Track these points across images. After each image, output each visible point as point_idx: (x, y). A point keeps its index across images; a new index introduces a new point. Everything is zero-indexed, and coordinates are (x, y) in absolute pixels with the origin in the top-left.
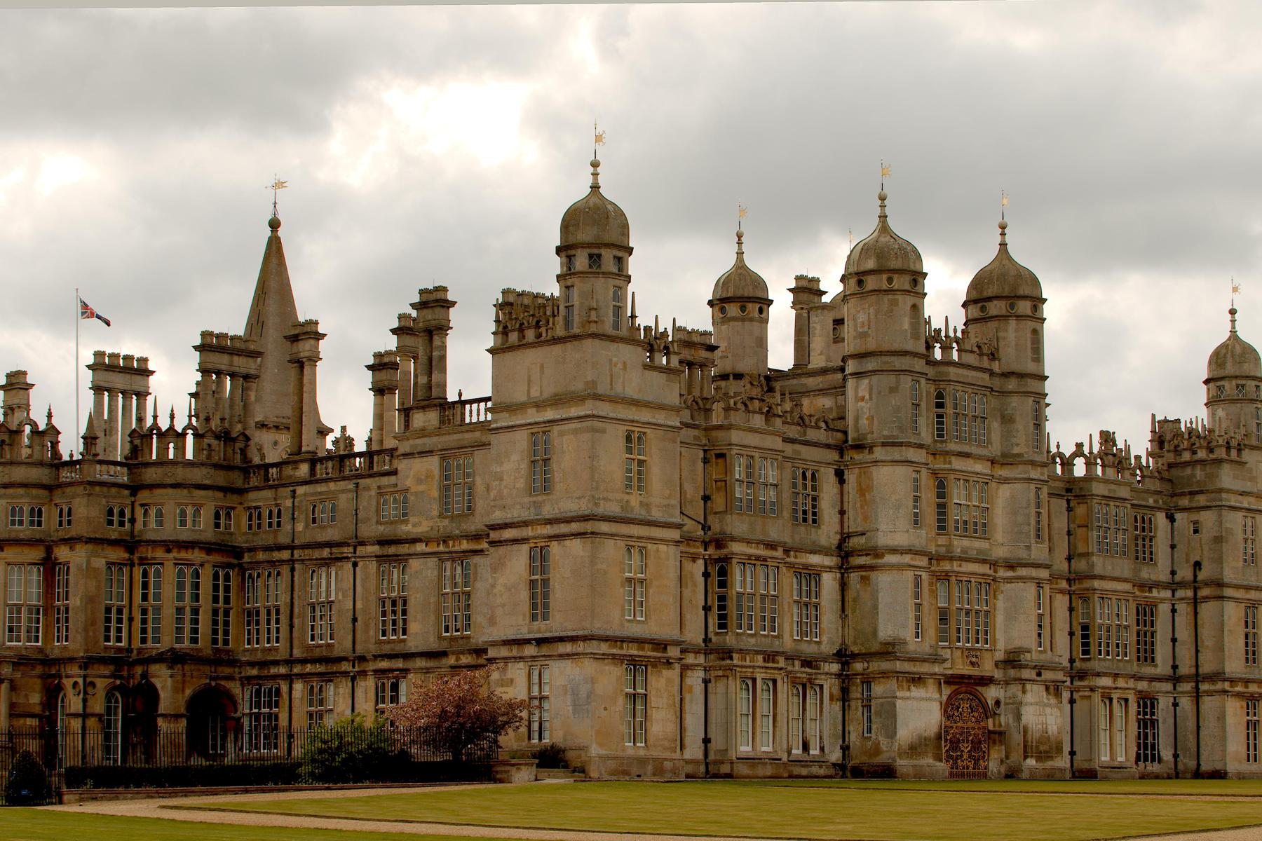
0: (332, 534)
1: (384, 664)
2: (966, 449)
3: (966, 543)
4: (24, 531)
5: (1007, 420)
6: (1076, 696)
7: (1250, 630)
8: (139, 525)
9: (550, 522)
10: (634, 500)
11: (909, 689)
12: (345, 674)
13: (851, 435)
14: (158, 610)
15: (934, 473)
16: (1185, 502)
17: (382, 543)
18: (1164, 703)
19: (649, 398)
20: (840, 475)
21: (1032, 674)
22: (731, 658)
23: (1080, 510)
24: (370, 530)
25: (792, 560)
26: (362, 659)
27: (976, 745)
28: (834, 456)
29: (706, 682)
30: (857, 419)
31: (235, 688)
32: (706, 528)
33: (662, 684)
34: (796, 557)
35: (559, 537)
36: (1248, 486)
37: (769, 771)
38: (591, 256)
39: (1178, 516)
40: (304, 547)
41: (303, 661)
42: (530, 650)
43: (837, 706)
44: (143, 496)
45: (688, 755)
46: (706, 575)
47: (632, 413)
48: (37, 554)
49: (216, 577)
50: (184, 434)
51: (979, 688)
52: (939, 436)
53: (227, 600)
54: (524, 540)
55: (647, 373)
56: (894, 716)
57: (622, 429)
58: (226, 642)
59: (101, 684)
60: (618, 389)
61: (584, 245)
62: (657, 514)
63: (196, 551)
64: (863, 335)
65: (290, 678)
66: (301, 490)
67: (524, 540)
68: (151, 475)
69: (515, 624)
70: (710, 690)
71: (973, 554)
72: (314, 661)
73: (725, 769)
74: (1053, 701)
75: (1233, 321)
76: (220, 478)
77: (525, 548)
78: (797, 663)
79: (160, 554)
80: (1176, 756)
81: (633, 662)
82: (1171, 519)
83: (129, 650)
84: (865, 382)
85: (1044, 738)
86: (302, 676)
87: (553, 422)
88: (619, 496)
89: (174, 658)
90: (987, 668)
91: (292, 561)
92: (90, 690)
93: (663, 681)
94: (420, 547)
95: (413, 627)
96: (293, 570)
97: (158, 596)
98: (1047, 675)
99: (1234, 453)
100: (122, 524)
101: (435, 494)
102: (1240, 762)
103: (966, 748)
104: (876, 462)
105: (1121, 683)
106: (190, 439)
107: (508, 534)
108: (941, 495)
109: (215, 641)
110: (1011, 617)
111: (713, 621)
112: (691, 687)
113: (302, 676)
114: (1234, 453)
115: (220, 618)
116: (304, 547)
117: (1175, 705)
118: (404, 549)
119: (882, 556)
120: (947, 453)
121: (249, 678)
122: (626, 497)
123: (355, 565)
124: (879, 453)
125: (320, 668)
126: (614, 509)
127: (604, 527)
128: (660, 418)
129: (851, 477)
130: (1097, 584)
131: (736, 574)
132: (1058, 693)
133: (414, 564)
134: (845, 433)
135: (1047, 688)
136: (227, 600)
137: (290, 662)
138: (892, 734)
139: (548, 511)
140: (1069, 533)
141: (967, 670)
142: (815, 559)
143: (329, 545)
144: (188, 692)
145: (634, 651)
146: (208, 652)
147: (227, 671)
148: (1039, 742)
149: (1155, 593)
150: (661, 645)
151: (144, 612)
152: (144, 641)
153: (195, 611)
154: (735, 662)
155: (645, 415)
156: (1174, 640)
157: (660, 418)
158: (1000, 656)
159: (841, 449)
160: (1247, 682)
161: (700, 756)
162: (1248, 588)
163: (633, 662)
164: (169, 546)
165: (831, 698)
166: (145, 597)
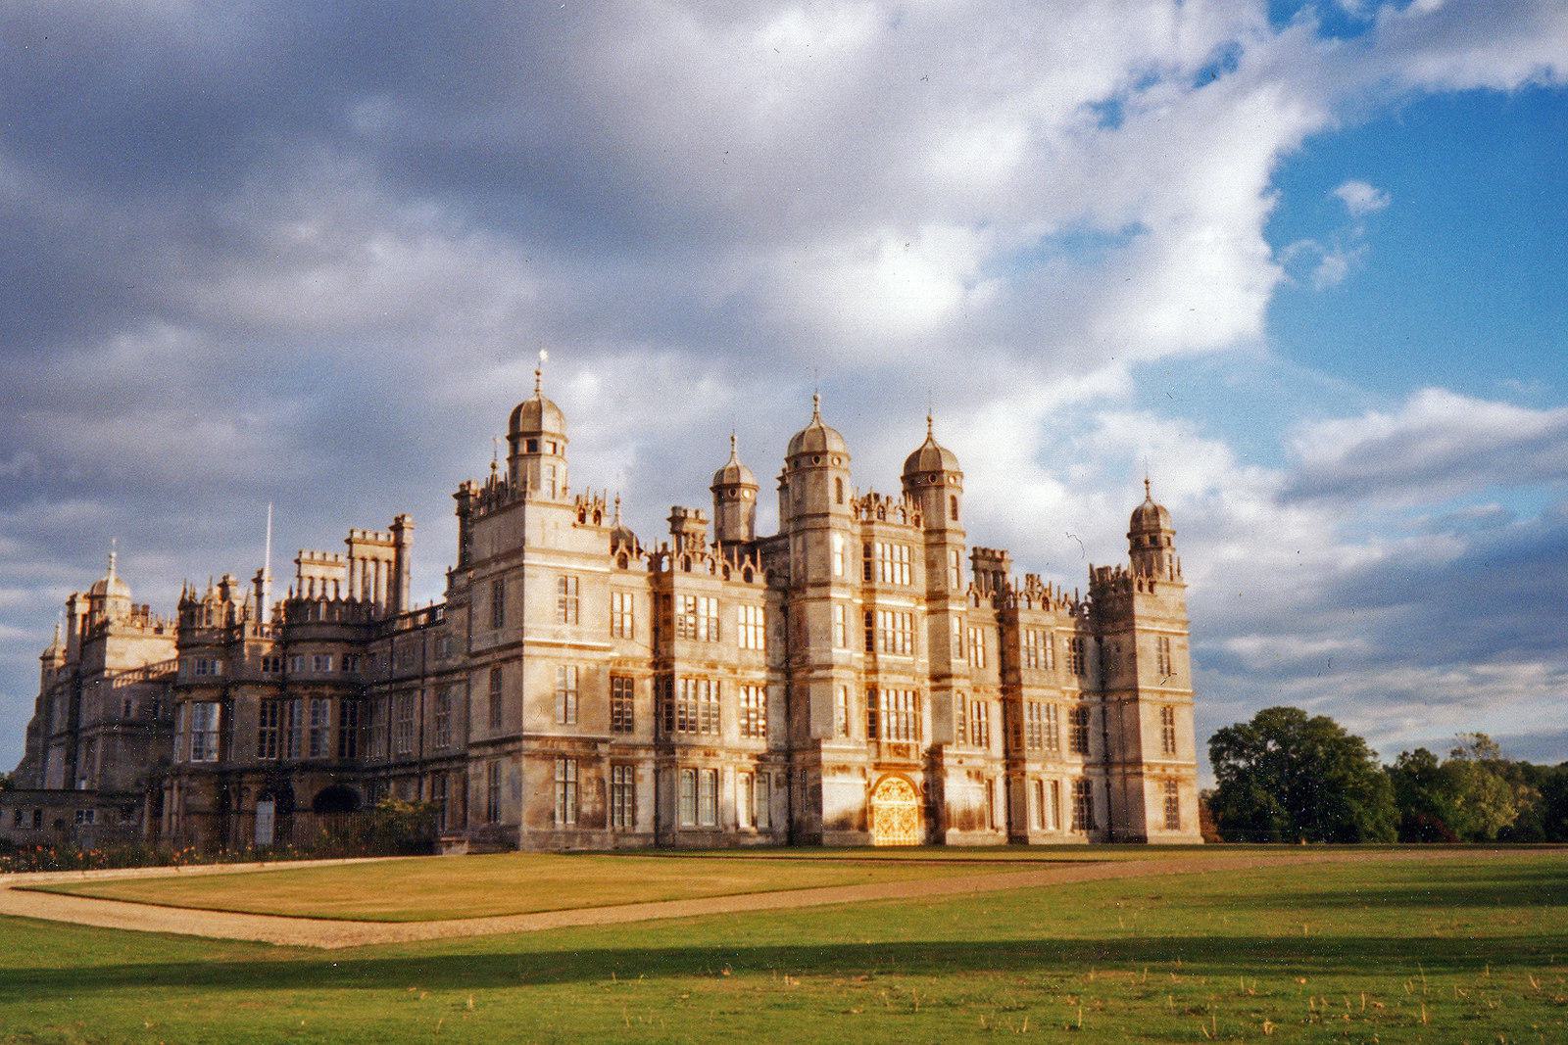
0: (408, 671)
1: (437, 767)
6: (1011, 779)
7: (1169, 727)
8: (289, 670)
9: (500, 649)
10: (567, 629)
11: (834, 774)
12: (413, 775)
13: (793, 580)
14: (300, 731)
16: (1109, 627)
17: (439, 674)
18: (1097, 785)
20: (784, 609)
22: (674, 753)
23: (1011, 635)
24: (432, 666)
25: (739, 676)
26: (424, 763)
28: (779, 595)
29: (656, 772)
30: (796, 567)
31: (360, 789)
34: (743, 674)
35: (506, 660)
36: (1161, 614)
37: (709, 842)
38: (529, 442)
39: (1106, 638)
40: (396, 681)
41: (396, 766)
42: (490, 751)
43: (783, 791)
44: (292, 649)
45: (639, 830)
46: (656, 688)
48: (215, 693)
49: (343, 706)
50: (318, 603)
51: (909, 774)
52: (866, 579)
54: (486, 665)
55: (580, 531)
56: (820, 794)
58: (352, 754)
59: (254, 789)
60: (550, 543)
61: (526, 434)
63: (327, 687)
64: (798, 503)
65: (387, 780)
66: (396, 639)
67: (486, 665)
68: (297, 633)
69: (480, 731)
70: (661, 778)
72: (403, 765)
73: (669, 839)
74: (975, 784)
75: (1147, 489)
76: (347, 634)
77: (488, 670)
78: (745, 757)
79: (300, 690)
80: (1110, 825)
82: (1099, 640)
83: (279, 762)
84: (800, 538)
85: (967, 814)
86: (394, 777)
87: (503, 572)
88: (550, 627)
89: (305, 767)
91: (390, 693)
92: (245, 793)
94: (457, 677)
95: (454, 737)
96: (391, 699)
97: (300, 723)
99: (1146, 588)
100: (275, 669)
101: (465, 635)
102: (1160, 829)
104: (806, 599)
106: (323, 607)
107: (478, 661)
109: (341, 754)
111: (662, 723)
112: (642, 776)
113: (394, 777)
114: (1146, 588)
115: (347, 737)
116: (396, 681)
117: (1108, 785)
118: (449, 678)
119: (811, 671)
121: (367, 780)
122: (558, 628)
123: (423, 692)
124: (811, 592)
125: (402, 771)
127: (536, 651)
128: (591, 566)
129: (793, 609)
133: (454, 689)
134: (789, 578)
135: (969, 773)
137: (387, 767)
138: (818, 807)
139: (501, 641)
143: (409, 678)
144: (315, 792)
147: (351, 776)
149: (1086, 698)
150: (592, 743)
151: (290, 733)
152: (289, 755)
154: (677, 756)
155: (575, 565)
156: (1105, 735)
157: (591, 566)
159: (786, 592)
160: (1164, 768)
161: (650, 829)
162: (1163, 693)
164: (307, 684)
165: (778, 781)
166: (291, 723)
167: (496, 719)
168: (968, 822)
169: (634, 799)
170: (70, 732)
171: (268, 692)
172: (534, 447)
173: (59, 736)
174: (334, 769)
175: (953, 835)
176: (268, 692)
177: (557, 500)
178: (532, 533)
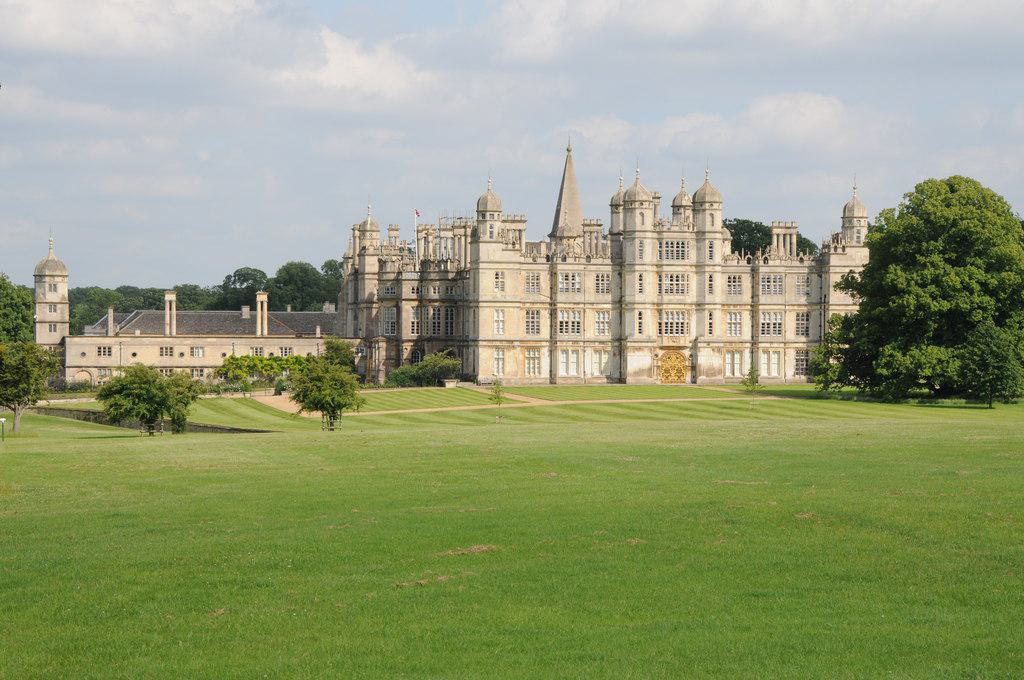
2: (672, 262)
3: (672, 297)
4: (388, 296)
5: (699, 249)
15: (657, 272)
19: (505, 260)
20: (620, 274)
21: (705, 345)
27: (679, 371)
32: (551, 298)
33: (509, 355)
45: (542, 376)
47: (497, 266)
48: (394, 303)
49: (447, 311)
53: (452, 319)
57: (494, 272)
60: (492, 258)
62: (509, 299)
71: (675, 301)
81: (497, 348)
90: (682, 344)
93: (511, 353)
98: (711, 345)
99: (840, 251)
103: (673, 373)
105: (775, 345)
108: (660, 280)
110: (700, 322)
114: (840, 251)
120: (662, 265)
126: (491, 299)
127: (485, 304)
128: (511, 266)
130: (760, 307)
131: (559, 314)
132: (719, 350)
136: (452, 319)
140: (753, 287)
141: (671, 344)
142: (605, 306)
145: (498, 344)
146: (444, 337)
148: (709, 369)
153: (439, 323)
155: (504, 266)
158: (693, 338)
163: (497, 348)
167: (474, 332)
168: (711, 372)
169: (539, 364)
170: (355, 303)
171: (415, 304)
172: (484, 216)
173: (351, 304)
174: (442, 340)
175: (701, 378)
176: (415, 304)
177: (494, 239)
178: (483, 256)
